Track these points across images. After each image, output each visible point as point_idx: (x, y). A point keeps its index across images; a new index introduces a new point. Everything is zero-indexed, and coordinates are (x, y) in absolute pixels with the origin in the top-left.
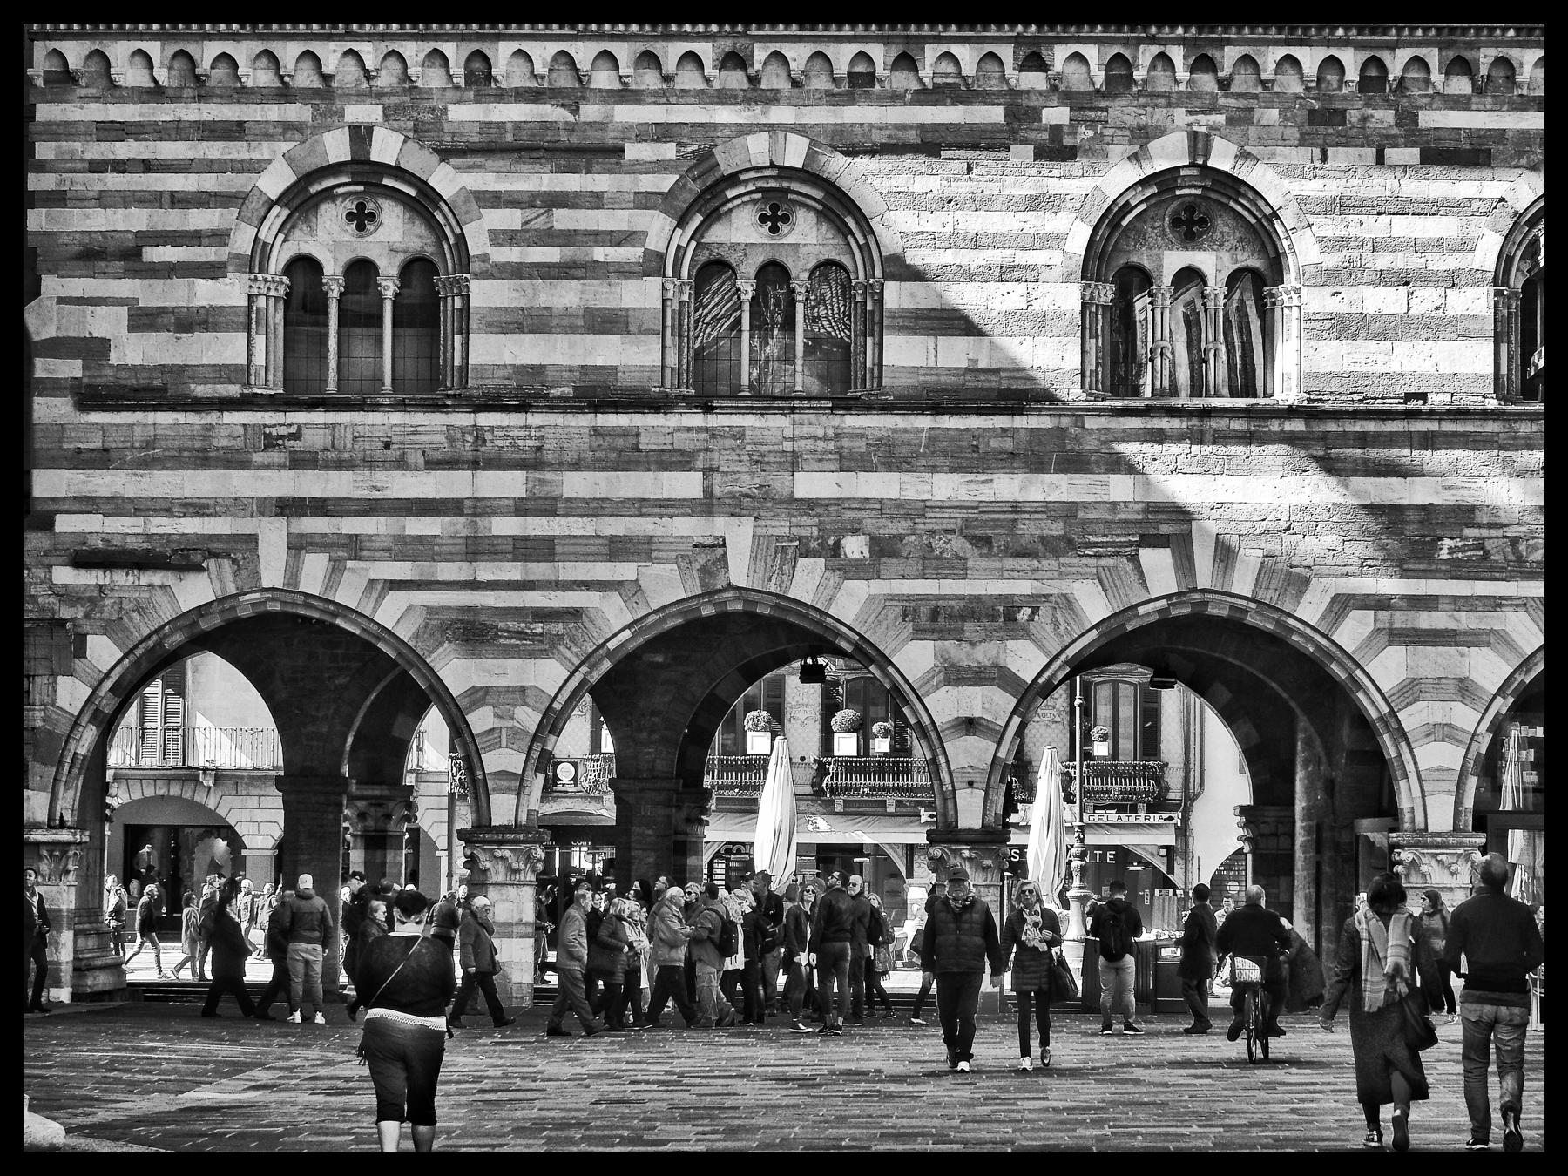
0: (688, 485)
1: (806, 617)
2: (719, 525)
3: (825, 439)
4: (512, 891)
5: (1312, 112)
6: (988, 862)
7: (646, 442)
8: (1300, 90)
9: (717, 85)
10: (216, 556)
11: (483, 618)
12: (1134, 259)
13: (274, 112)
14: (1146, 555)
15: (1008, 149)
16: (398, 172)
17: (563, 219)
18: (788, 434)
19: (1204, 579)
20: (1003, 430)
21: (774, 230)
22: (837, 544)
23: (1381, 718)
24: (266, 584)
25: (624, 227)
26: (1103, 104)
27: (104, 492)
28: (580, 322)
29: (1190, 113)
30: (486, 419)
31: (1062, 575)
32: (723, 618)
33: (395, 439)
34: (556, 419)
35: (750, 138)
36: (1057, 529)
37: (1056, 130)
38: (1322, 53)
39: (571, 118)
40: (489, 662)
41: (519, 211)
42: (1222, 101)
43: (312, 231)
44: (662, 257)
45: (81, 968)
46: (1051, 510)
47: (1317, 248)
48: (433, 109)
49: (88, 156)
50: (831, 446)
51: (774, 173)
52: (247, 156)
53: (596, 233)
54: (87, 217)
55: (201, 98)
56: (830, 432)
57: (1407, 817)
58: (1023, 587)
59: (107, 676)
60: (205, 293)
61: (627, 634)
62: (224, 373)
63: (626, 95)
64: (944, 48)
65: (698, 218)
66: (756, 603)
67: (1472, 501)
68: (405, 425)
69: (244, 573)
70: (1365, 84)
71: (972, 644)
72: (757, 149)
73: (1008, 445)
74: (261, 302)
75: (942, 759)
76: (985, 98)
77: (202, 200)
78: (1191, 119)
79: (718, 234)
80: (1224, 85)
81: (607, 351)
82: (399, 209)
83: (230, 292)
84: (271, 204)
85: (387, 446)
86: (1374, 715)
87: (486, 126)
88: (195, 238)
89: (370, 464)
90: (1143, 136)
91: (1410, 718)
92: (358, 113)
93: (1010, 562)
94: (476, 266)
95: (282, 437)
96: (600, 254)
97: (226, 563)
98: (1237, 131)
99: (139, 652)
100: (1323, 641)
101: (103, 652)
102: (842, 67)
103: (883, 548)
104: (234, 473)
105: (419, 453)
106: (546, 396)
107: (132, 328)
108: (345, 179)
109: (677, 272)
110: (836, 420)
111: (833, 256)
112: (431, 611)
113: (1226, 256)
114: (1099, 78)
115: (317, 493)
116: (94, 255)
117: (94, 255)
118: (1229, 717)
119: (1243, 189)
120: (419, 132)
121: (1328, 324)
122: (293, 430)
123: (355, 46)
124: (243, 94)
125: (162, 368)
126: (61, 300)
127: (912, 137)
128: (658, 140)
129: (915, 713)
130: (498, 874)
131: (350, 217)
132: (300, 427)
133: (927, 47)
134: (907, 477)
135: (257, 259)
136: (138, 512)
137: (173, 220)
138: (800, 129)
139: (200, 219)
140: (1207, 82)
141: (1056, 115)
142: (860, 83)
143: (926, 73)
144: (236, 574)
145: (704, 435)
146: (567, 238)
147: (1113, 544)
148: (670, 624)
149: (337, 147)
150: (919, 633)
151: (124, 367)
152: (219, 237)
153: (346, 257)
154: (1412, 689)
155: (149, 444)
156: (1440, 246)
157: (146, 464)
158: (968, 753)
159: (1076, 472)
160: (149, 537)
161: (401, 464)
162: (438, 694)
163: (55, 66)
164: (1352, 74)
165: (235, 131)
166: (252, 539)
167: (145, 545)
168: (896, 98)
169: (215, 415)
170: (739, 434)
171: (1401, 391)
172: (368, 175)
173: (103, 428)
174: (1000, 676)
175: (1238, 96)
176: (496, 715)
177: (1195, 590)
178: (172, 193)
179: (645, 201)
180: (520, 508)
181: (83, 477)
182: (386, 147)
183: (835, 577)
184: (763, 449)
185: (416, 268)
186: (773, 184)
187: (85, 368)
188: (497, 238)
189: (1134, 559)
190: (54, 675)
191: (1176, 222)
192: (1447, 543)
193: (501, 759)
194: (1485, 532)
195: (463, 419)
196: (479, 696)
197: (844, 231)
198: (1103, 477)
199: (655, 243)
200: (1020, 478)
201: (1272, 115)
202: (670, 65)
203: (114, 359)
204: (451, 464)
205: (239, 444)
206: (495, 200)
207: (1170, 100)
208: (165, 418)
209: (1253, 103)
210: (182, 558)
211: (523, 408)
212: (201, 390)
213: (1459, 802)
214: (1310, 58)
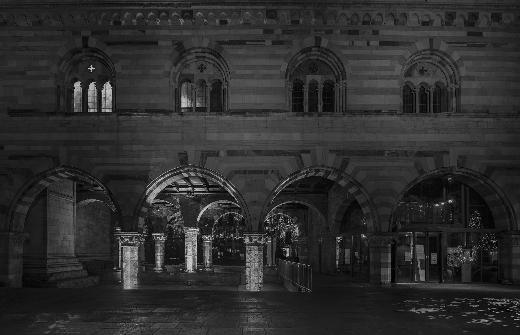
14: (303, 155)
15: (264, 41)
16: (96, 51)
29: (315, 31)
44: (169, 73)
51: (200, 50)
72: (195, 42)
78: (316, 33)
84: (62, 60)
85: (94, 126)
119: (330, 54)
122: (68, 122)
132: (70, 121)
156: (385, 68)
182: (93, 43)
186: (200, 54)
189: (300, 156)
213: (390, 224)
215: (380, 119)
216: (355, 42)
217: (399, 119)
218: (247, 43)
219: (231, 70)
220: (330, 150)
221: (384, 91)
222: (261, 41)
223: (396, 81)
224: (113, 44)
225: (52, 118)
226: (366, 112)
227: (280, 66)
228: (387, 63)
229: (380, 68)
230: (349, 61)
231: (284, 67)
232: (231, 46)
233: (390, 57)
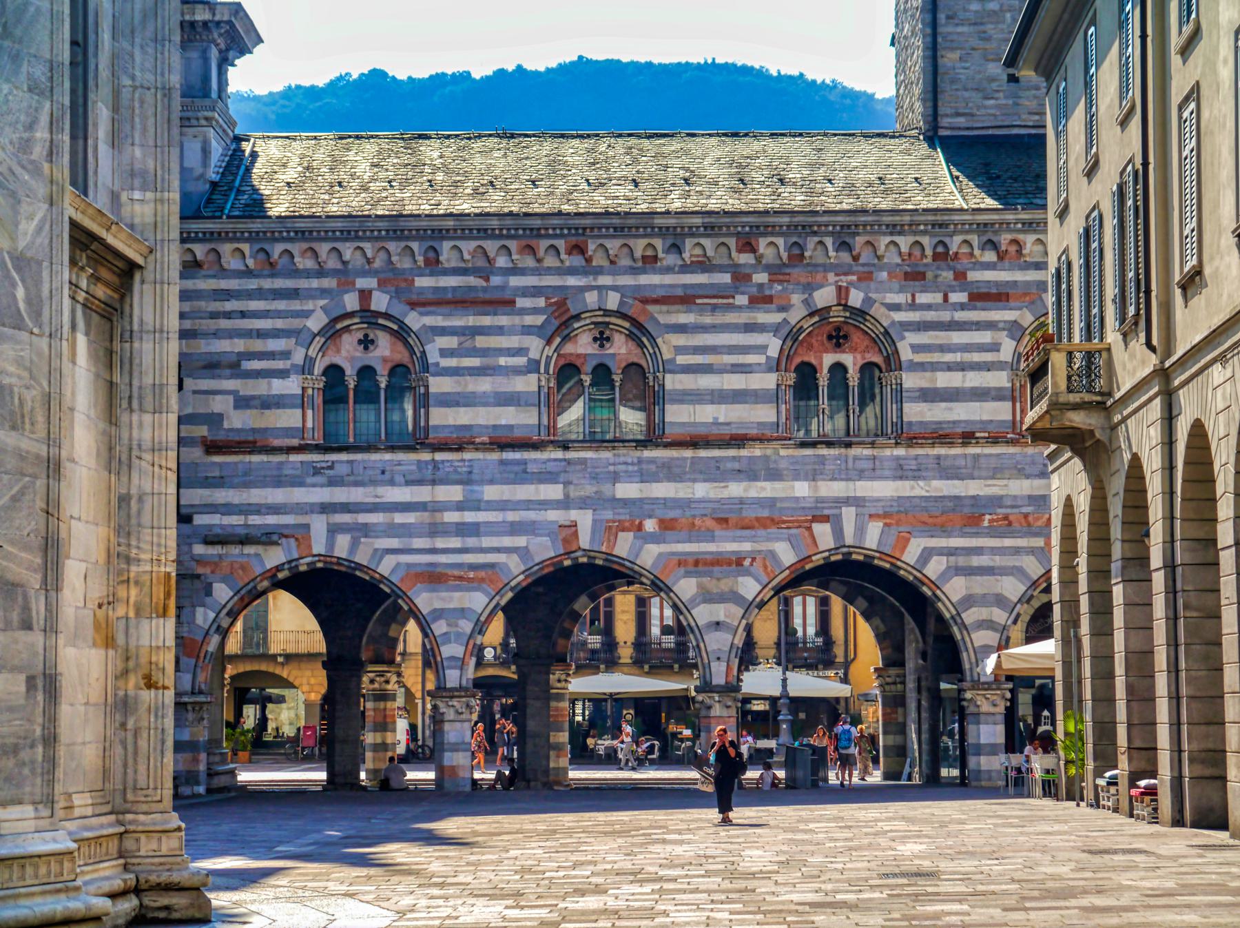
0: (553, 491)
1: (623, 565)
2: (574, 515)
3: (633, 464)
4: (458, 725)
5: (906, 273)
6: (729, 703)
7: (531, 468)
8: (899, 261)
9: (567, 264)
10: (286, 537)
11: (439, 570)
12: (806, 359)
13: (315, 283)
16: (387, 316)
17: (481, 342)
18: (611, 461)
19: (849, 540)
20: (734, 457)
21: (602, 346)
22: (641, 523)
23: (952, 617)
24: (315, 551)
25: (516, 345)
26: (787, 270)
27: (222, 501)
28: (492, 400)
29: (837, 275)
30: (439, 456)
31: (769, 539)
32: (577, 566)
34: (480, 455)
35: (587, 294)
36: (765, 513)
37: (761, 286)
38: (911, 239)
39: (485, 284)
40: (444, 594)
42: (855, 269)
43: (338, 351)
44: (538, 362)
45: (211, 774)
46: (760, 502)
47: (910, 350)
48: (406, 280)
49: (209, 309)
50: (636, 468)
53: (500, 350)
54: (208, 344)
55: (272, 276)
56: (635, 461)
57: (968, 673)
58: (747, 547)
59: (224, 606)
60: (279, 387)
61: (522, 577)
62: (288, 432)
63: (515, 271)
64: (696, 240)
65: (558, 340)
66: (595, 558)
67: (1001, 493)
69: (302, 546)
70: (936, 256)
71: (718, 579)
72: (591, 298)
73: (736, 466)
74: (310, 391)
75: (702, 645)
76: (721, 269)
79: (569, 348)
80: (856, 258)
81: (508, 417)
82: (388, 336)
83: (291, 386)
85: (383, 472)
86: (948, 615)
87: (436, 289)
88: (271, 355)
89: (373, 483)
90: (809, 288)
91: (970, 617)
92: (362, 283)
93: (739, 533)
94: (431, 369)
96: (502, 361)
97: (292, 541)
98: (863, 285)
99: (243, 592)
100: (918, 575)
101: (222, 593)
102: (638, 254)
103: (667, 525)
106: (473, 443)
107: (236, 407)
108: (356, 320)
109: (547, 372)
110: (638, 454)
111: (635, 360)
112: (409, 565)
113: (859, 356)
114: (785, 255)
118: (867, 616)
120: (397, 294)
121: (917, 394)
123: (361, 245)
124: (295, 273)
125: (253, 430)
126: (195, 392)
127: (680, 292)
128: (534, 296)
129: (686, 619)
130: (450, 714)
131: (360, 342)
133: (687, 240)
134: (679, 485)
135: (306, 368)
136: (240, 513)
137: (258, 345)
138: (615, 288)
140: (845, 257)
141: (761, 278)
142: (650, 261)
143: (686, 255)
144: (298, 546)
145: (563, 463)
146: (484, 353)
147: (797, 521)
148: (546, 571)
150: (688, 574)
151: (231, 430)
152: (286, 355)
153: (359, 365)
154: (969, 601)
155: (245, 474)
156: (982, 348)
157: (247, 485)
158: (717, 642)
159: (774, 480)
160: (246, 526)
161: (392, 483)
162: (414, 613)
164: (929, 252)
165: (294, 294)
166: (307, 527)
168: (669, 270)
170: (583, 461)
171: (959, 430)
172: (368, 315)
173: (220, 465)
174: (735, 598)
175: (863, 265)
176: (448, 625)
177: (845, 546)
178: (258, 330)
179: (527, 330)
180: (460, 507)
182: (380, 302)
183: (638, 543)
184: (598, 470)
185: (398, 370)
186: (600, 319)
187: (209, 430)
188: (444, 353)
189: (809, 529)
190: (194, 606)
191: (830, 337)
192: (988, 517)
193: (451, 650)
194: (1009, 511)
195: (426, 456)
196: (439, 614)
197: (641, 345)
198: (791, 483)
199: (534, 354)
200: (745, 484)
201: (885, 274)
202: (541, 253)
203: (226, 425)
204: (420, 482)
205: (298, 472)
206: (443, 331)
207: (826, 268)
208: (256, 458)
209: (872, 269)
210: (268, 538)
211: (460, 449)
212: (277, 443)
214: (904, 242)
215: (972, 450)
216: (917, 295)
217: (1011, 450)
218: (698, 301)
219: (666, 356)
220: (871, 516)
221: (980, 394)
222: (727, 297)
223: (1004, 373)
224: (424, 304)
225: (294, 458)
226: (940, 436)
227: (766, 347)
228: (985, 337)
229: (967, 348)
230: (907, 334)
231: (774, 346)
232: (664, 308)
233: (991, 326)
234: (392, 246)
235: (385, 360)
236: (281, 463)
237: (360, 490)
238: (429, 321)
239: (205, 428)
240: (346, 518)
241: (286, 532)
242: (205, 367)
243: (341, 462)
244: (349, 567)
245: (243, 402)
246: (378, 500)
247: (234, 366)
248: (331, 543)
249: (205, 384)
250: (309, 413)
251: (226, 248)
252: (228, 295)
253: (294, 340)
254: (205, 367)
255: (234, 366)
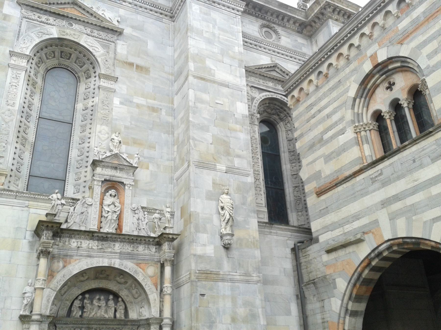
13: (347, 70)
16: (390, 60)
24: (386, 239)
27: (330, 222)
33: (416, 157)
41: (435, 41)
52: (344, 89)
60: (342, 139)
62: (352, 163)
68: (418, 149)
74: (363, 133)
77: (334, 112)
85: (414, 161)
87: (413, 22)
89: (410, 171)
92: (369, 52)
95: (376, 177)
97: (370, 234)
99: (353, 281)
104: (365, 198)
105: (428, 158)
107: (326, 162)
108: (377, 76)
115: (394, 193)
116: (312, 147)
117: (312, 147)
122: (379, 172)
125: (336, 172)
126: (308, 165)
131: (387, 88)
132: (381, 170)
137: (329, 122)
139: (335, 118)
149: (368, 67)
152: (342, 119)
157: (339, 208)
160: (345, 234)
161: (422, 166)
163: (294, 100)
166: (376, 222)
167: (345, 238)
169: (354, 179)
181: (323, 220)
188: (430, 57)
203: (323, 175)
208: (340, 188)
212: (347, 173)
234: (379, 19)
235: (403, 89)
236: (353, 185)
237: (403, 181)
238: (413, 44)
239: (315, 182)
240: (397, 206)
241: (366, 230)
242: (309, 150)
243: (387, 167)
244: (413, 243)
245: (328, 158)
246: (416, 183)
247: (320, 141)
248: (394, 229)
249: (310, 158)
250: (366, 147)
251: (305, 85)
252: (311, 106)
253: (344, 108)
254: (309, 150)
255: (320, 141)
